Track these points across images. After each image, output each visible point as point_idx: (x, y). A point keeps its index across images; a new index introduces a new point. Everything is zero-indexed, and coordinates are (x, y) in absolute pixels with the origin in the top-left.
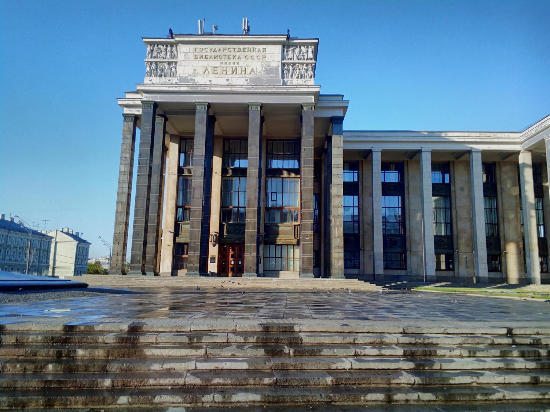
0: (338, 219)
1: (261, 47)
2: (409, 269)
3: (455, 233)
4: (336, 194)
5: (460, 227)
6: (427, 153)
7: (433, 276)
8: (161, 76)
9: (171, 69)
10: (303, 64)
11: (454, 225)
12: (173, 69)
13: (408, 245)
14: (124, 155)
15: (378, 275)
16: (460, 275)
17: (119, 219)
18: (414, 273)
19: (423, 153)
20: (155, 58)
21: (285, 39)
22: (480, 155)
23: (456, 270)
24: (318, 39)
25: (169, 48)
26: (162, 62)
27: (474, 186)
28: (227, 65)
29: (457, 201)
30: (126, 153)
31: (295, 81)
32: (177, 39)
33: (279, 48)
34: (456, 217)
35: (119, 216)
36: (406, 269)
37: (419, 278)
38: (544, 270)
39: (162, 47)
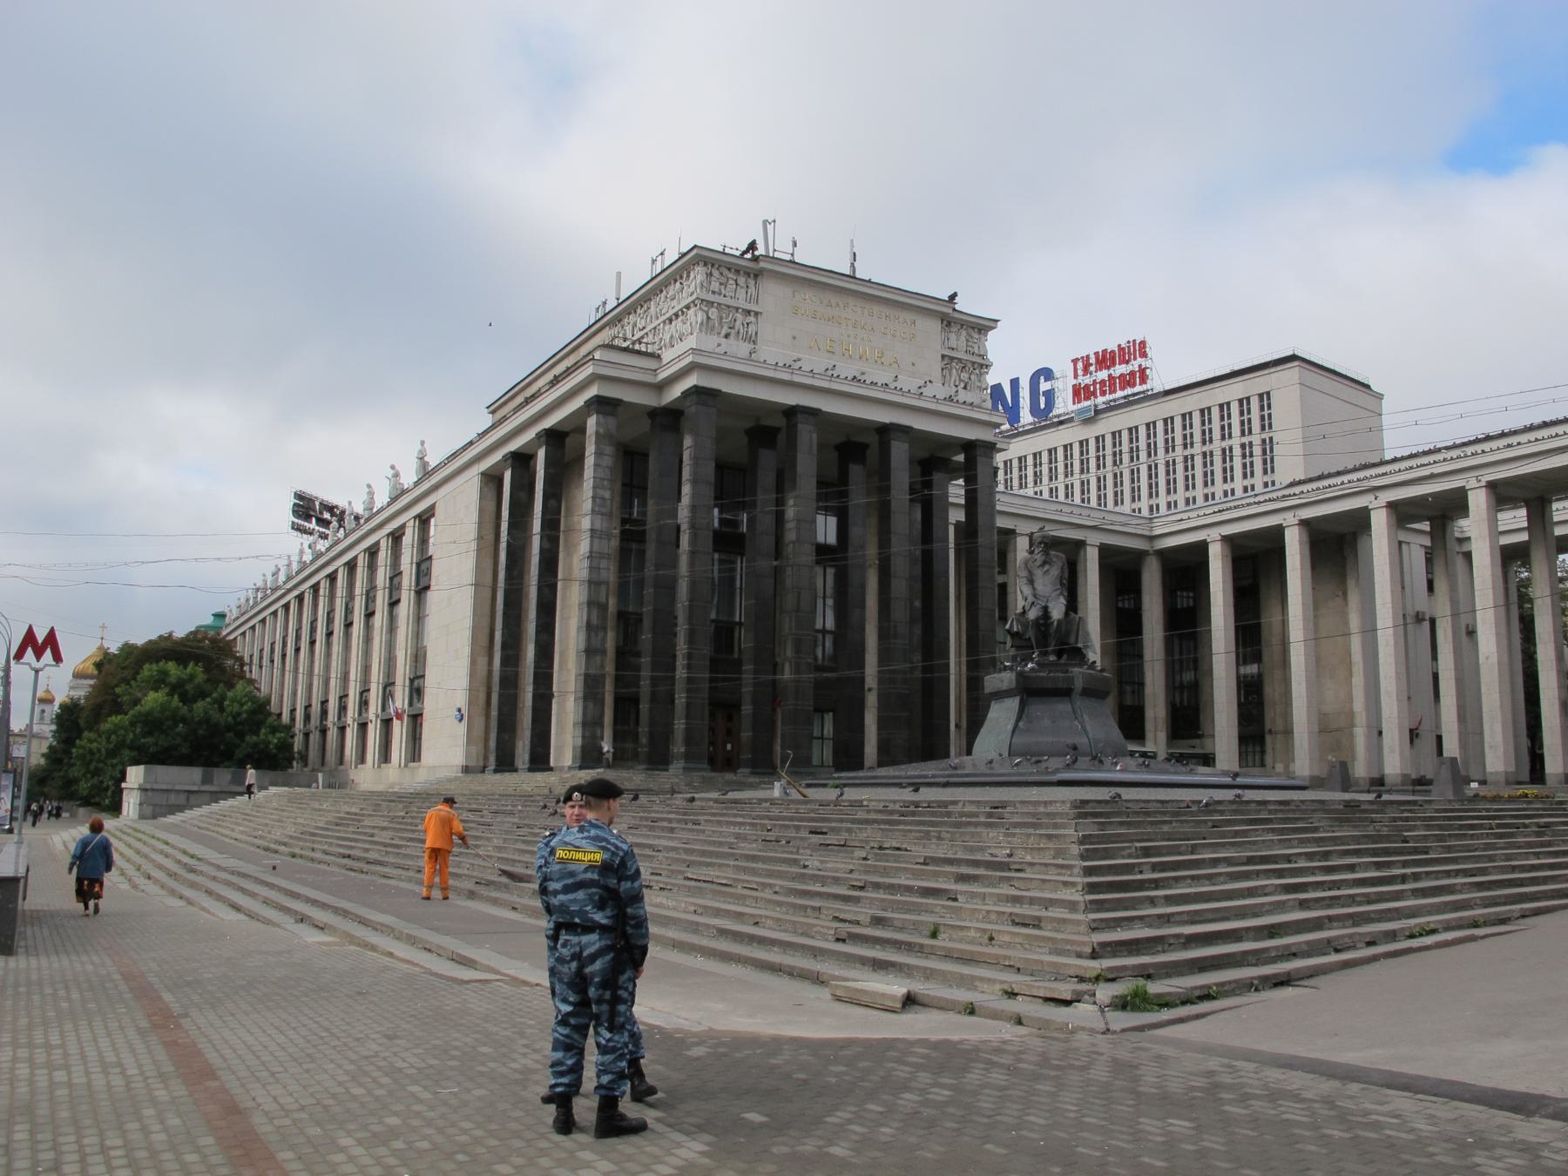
8: (727, 336)
12: (752, 329)
14: (600, 492)
25: (741, 281)
30: (603, 488)
31: (963, 396)
32: (762, 265)
39: (726, 272)
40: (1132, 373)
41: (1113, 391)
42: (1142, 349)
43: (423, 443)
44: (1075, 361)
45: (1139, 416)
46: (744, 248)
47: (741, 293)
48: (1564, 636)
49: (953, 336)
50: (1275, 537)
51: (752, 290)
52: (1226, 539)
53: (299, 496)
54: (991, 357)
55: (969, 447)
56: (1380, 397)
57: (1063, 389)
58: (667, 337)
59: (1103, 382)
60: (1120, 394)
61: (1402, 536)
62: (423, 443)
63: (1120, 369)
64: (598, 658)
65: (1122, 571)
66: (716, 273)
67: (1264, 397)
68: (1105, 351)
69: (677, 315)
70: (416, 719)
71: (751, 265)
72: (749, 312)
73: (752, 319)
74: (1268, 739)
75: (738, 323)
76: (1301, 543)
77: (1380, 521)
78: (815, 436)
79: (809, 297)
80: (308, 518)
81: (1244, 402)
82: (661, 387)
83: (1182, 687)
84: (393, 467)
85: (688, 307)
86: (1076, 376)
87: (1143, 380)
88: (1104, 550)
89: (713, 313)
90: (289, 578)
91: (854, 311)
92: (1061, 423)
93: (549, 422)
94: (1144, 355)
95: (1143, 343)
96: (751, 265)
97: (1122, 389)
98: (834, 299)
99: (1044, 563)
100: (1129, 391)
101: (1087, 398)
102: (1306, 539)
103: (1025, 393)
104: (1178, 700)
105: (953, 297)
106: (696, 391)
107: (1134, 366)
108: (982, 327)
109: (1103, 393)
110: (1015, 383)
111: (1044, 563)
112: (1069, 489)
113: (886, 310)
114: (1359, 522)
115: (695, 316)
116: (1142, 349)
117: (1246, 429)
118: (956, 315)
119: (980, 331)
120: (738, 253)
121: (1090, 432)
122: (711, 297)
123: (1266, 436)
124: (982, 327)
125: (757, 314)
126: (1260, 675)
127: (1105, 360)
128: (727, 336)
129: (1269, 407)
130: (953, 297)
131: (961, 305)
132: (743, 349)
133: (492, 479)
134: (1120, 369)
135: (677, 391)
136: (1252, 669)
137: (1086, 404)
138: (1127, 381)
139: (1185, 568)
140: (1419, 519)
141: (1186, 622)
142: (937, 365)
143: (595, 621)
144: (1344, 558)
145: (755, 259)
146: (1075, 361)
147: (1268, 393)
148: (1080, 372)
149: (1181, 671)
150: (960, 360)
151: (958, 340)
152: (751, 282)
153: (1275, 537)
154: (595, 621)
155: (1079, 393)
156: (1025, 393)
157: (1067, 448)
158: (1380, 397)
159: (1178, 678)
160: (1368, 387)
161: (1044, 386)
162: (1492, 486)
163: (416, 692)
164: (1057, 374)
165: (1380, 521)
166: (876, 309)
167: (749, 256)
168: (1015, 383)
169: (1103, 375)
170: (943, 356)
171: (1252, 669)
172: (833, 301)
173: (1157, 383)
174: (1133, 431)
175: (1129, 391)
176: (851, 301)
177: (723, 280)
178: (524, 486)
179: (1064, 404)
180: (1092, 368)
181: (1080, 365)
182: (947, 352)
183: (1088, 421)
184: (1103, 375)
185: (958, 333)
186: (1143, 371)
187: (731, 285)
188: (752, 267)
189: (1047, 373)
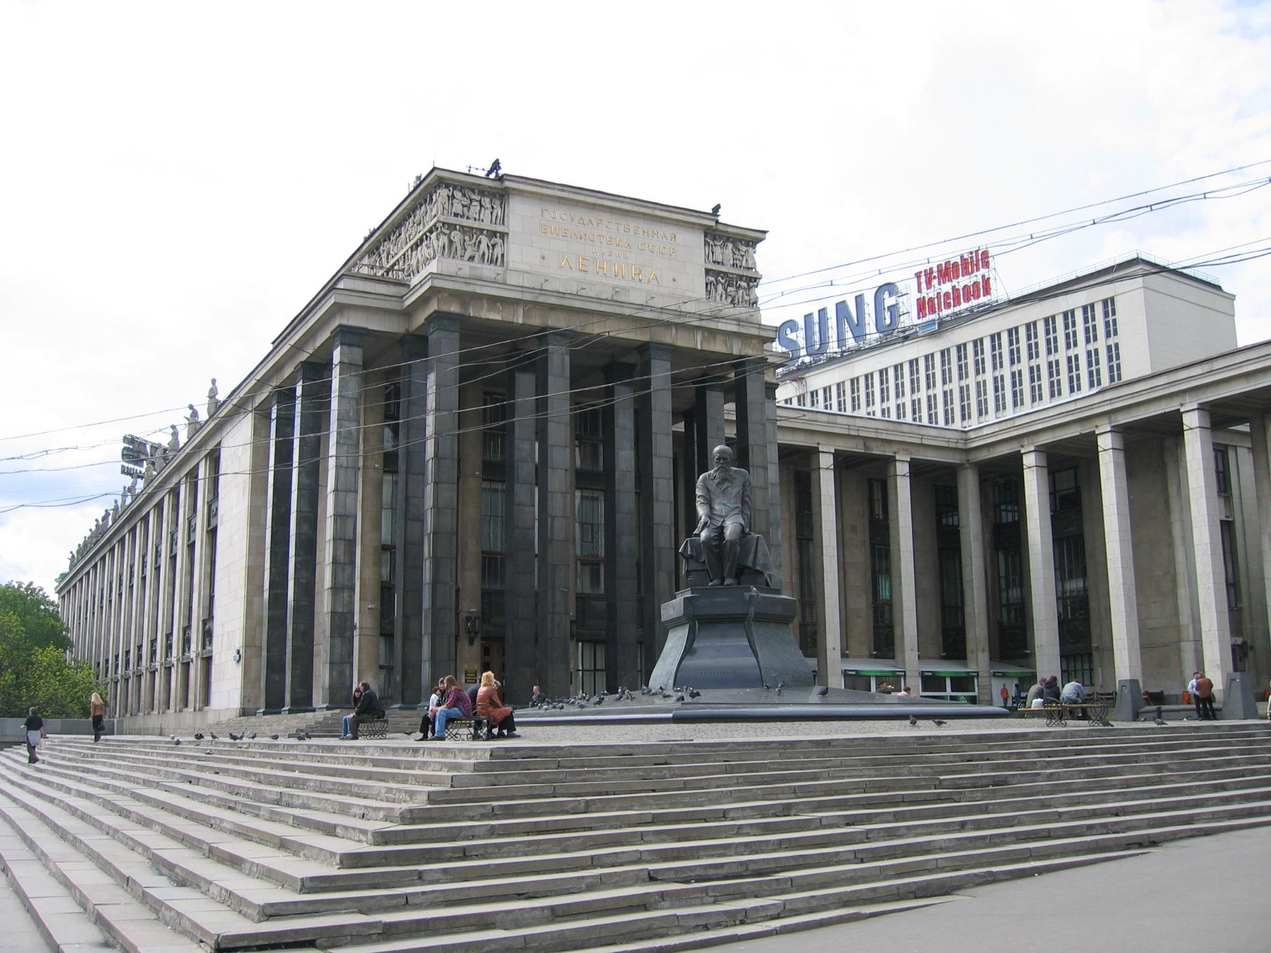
1: (669, 230)
8: (472, 258)
9: (493, 246)
10: (741, 277)
12: (498, 251)
17: (340, 578)
20: (456, 215)
21: (713, 224)
24: (765, 232)
25: (486, 201)
26: (472, 228)
28: (606, 257)
30: (349, 420)
31: (731, 311)
32: (507, 184)
33: (699, 238)
35: (339, 571)
40: (976, 284)
41: (957, 303)
42: (983, 258)
43: (214, 381)
44: (918, 275)
45: (984, 328)
46: (488, 168)
47: (486, 215)
49: (718, 250)
51: (498, 211)
53: (130, 440)
54: (761, 268)
55: (740, 364)
56: (1232, 298)
57: (909, 305)
58: (414, 262)
59: (947, 295)
60: (964, 306)
61: (1223, 439)
62: (214, 381)
63: (963, 281)
64: (346, 594)
65: (937, 483)
66: (458, 194)
67: (1109, 304)
68: (947, 263)
69: (421, 240)
70: (208, 660)
71: (497, 184)
72: (493, 234)
73: (499, 240)
75: (483, 247)
78: (567, 358)
79: (559, 215)
80: (139, 462)
81: (1088, 309)
82: (408, 313)
83: (1008, 606)
84: (191, 407)
85: (431, 231)
86: (920, 291)
87: (987, 291)
88: (915, 466)
89: (456, 236)
90: (115, 521)
91: (609, 226)
92: (906, 338)
93: (304, 357)
94: (986, 265)
95: (985, 254)
96: (497, 184)
97: (967, 300)
98: (586, 215)
99: (724, 480)
100: (974, 302)
101: (932, 311)
103: (870, 310)
105: (717, 209)
106: (438, 316)
107: (977, 277)
108: (749, 239)
109: (948, 306)
110: (859, 300)
111: (724, 480)
112: (915, 405)
113: (642, 225)
114: (1171, 427)
115: (437, 242)
116: (983, 258)
117: (1090, 336)
118: (720, 227)
119: (748, 245)
120: (483, 174)
121: (933, 346)
122: (453, 220)
123: (1111, 341)
124: (749, 239)
125: (503, 235)
126: (1085, 590)
127: (947, 272)
128: (472, 258)
129: (1114, 314)
130: (717, 209)
131: (724, 217)
132: (488, 271)
133: (262, 414)
134: (963, 281)
135: (420, 319)
136: (1075, 585)
137: (930, 317)
138: (970, 292)
139: (1001, 478)
140: (1242, 421)
141: (1007, 539)
142: (701, 280)
143: (342, 558)
145: (500, 179)
146: (918, 275)
147: (1112, 299)
148: (924, 286)
149: (1007, 588)
150: (726, 274)
151: (725, 253)
152: (498, 202)
154: (342, 558)
155: (921, 305)
156: (870, 310)
157: (913, 363)
158: (1232, 298)
159: (1004, 595)
160: (1219, 288)
161: (889, 301)
163: (208, 635)
164: (901, 287)
166: (632, 224)
167: (492, 176)
168: (859, 300)
169: (947, 287)
170: (708, 272)
171: (1075, 585)
172: (586, 220)
173: (1000, 293)
174: (978, 343)
175: (974, 302)
176: (605, 217)
177: (466, 202)
178: (285, 423)
179: (910, 319)
180: (935, 282)
181: (923, 279)
182: (709, 267)
183: (932, 335)
184: (947, 287)
185: (724, 246)
186: (986, 282)
187: (475, 207)
188: (498, 189)
189: (889, 287)
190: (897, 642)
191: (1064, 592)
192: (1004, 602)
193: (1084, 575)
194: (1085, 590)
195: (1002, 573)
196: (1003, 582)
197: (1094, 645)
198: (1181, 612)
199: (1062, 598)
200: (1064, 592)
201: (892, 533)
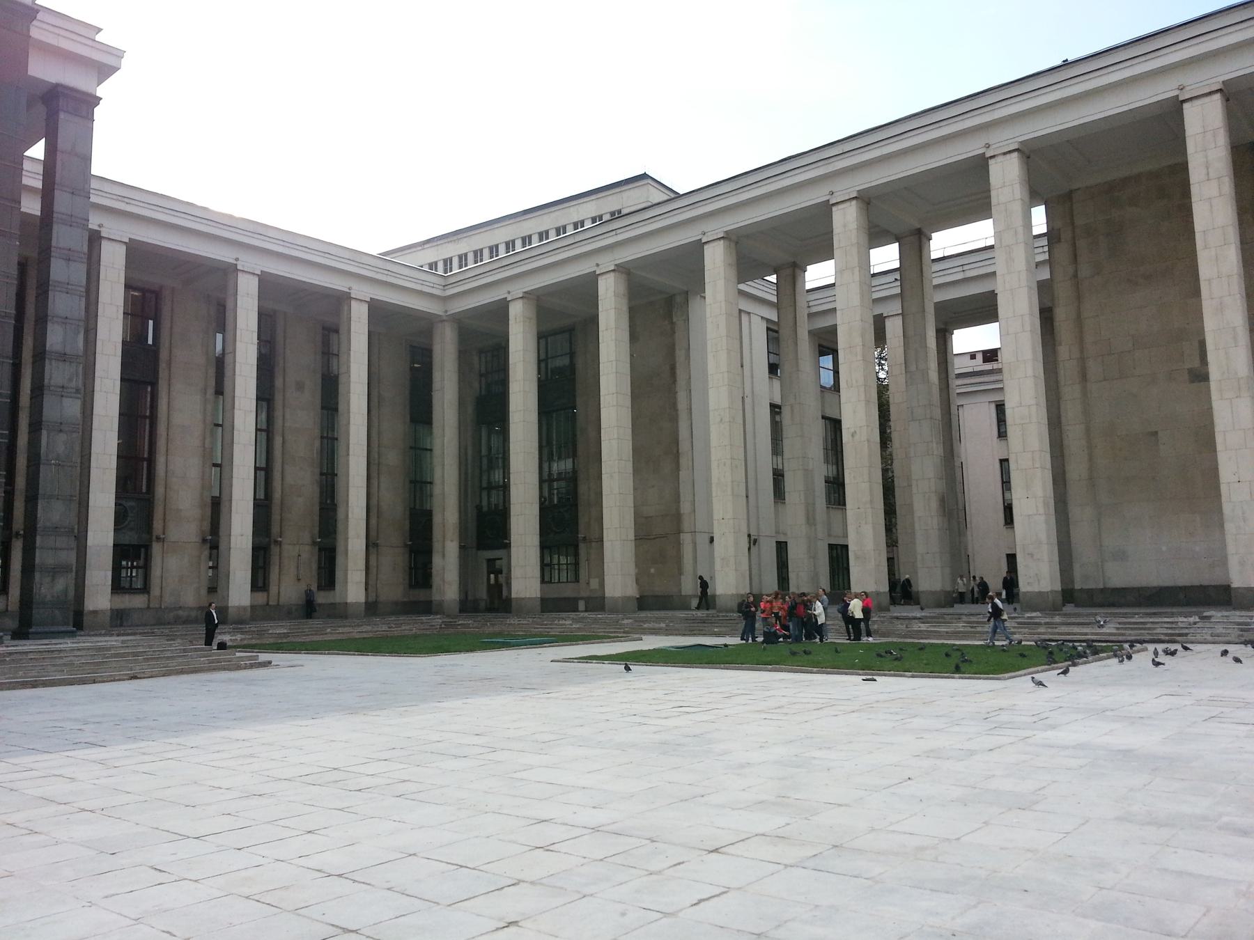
0: (62, 437)
2: (155, 591)
3: (277, 495)
4: (58, 348)
5: (289, 479)
6: (251, 277)
7: (245, 608)
11: (277, 475)
13: (157, 526)
15: (95, 612)
16: (282, 601)
18: (168, 600)
19: (240, 274)
22: (365, 308)
23: (273, 589)
27: (349, 382)
29: (288, 416)
34: (283, 454)
36: (145, 589)
37: (180, 612)
38: (547, 579)
48: (1250, 210)
50: (586, 288)
52: (527, 296)
74: (582, 546)
76: (616, 295)
77: (716, 260)
102: (622, 289)
104: (485, 503)
126: (575, 471)
136: (562, 466)
141: (489, 409)
144: (672, 323)
153: (586, 288)
159: (485, 477)
162: (866, 199)
165: (716, 260)
171: (562, 466)
190: (340, 526)
191: (550, 474)
192: (484, 484)
193: (574, 455)
194: (575, 471)
195: (484, 452)
196: (485, 461)
197: (581, 536)
198: (682, 499)
199: (545, 480)
200: (550, 474)
201: (341, 389)
